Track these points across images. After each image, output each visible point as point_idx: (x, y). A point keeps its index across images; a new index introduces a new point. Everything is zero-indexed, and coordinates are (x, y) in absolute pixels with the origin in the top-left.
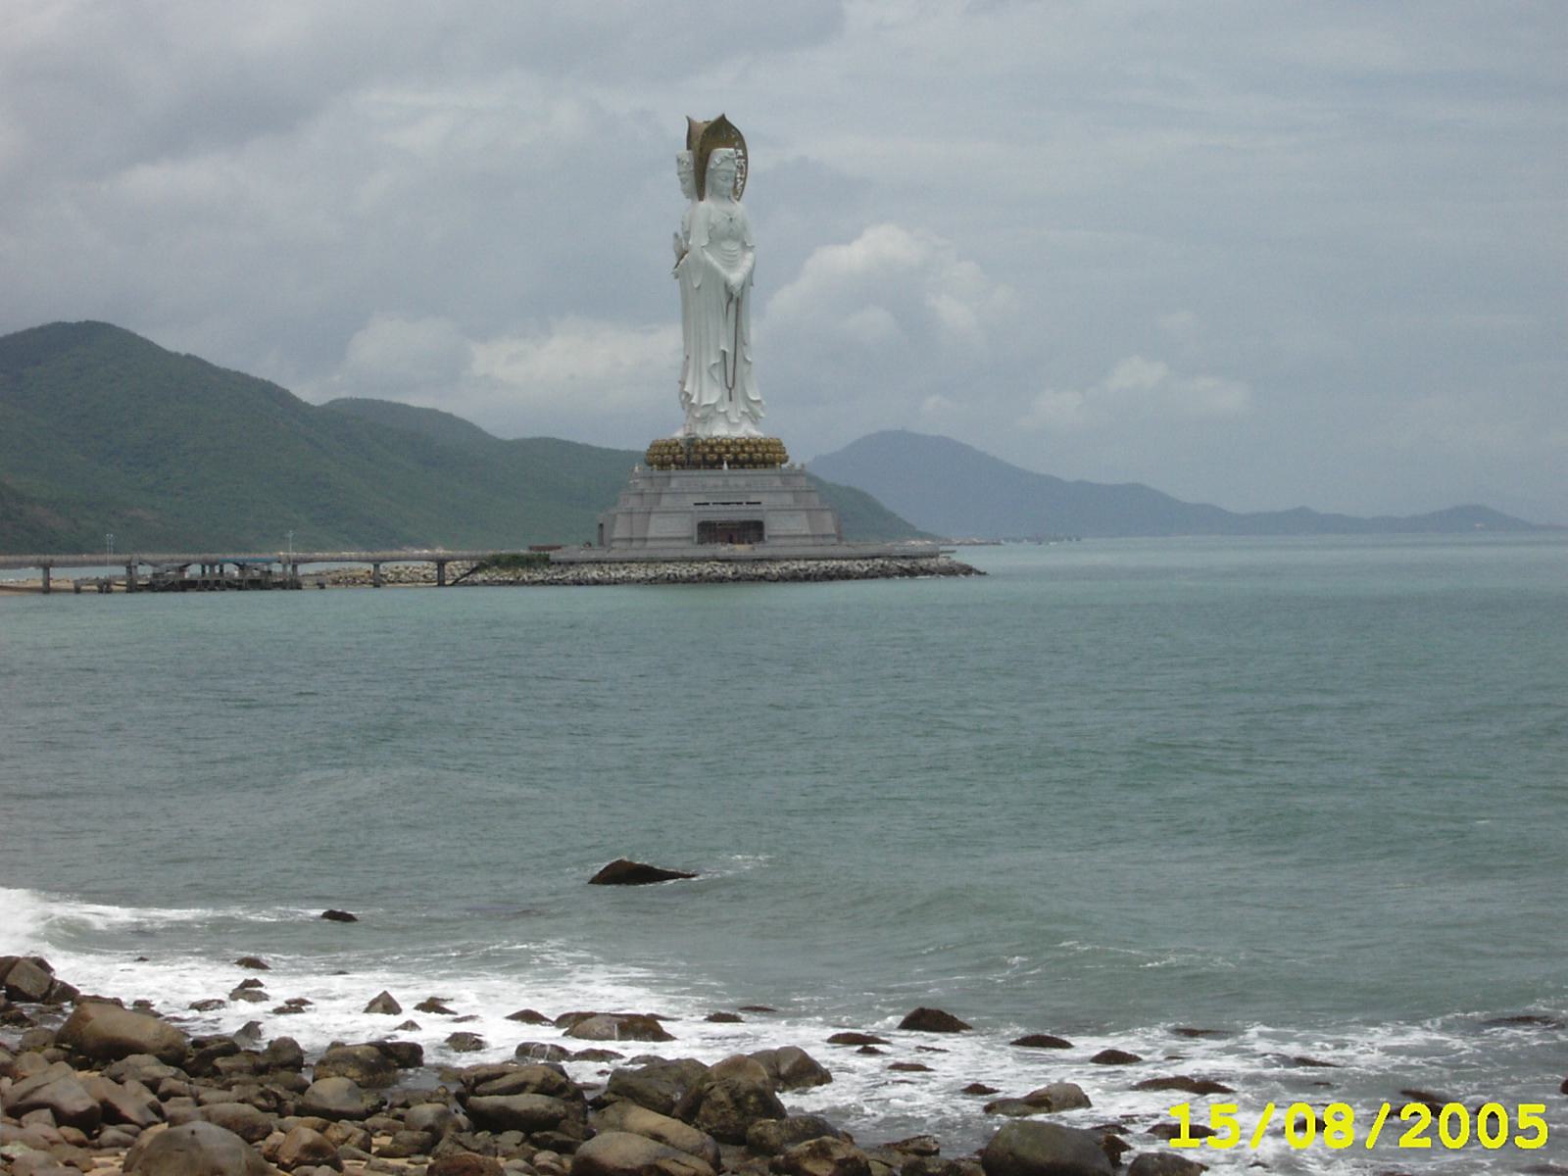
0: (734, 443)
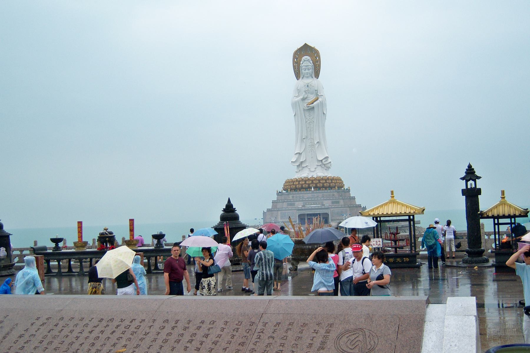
0: (322, 179)
